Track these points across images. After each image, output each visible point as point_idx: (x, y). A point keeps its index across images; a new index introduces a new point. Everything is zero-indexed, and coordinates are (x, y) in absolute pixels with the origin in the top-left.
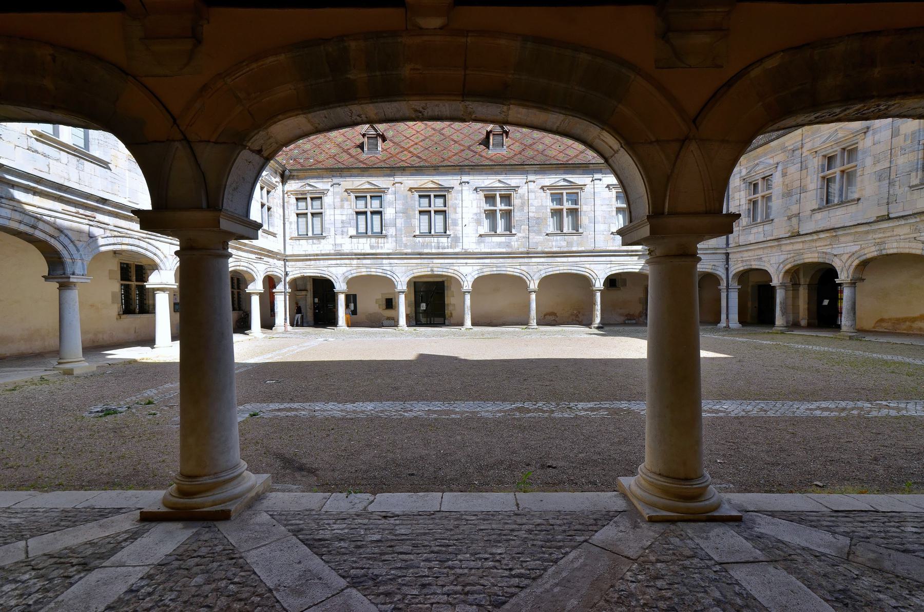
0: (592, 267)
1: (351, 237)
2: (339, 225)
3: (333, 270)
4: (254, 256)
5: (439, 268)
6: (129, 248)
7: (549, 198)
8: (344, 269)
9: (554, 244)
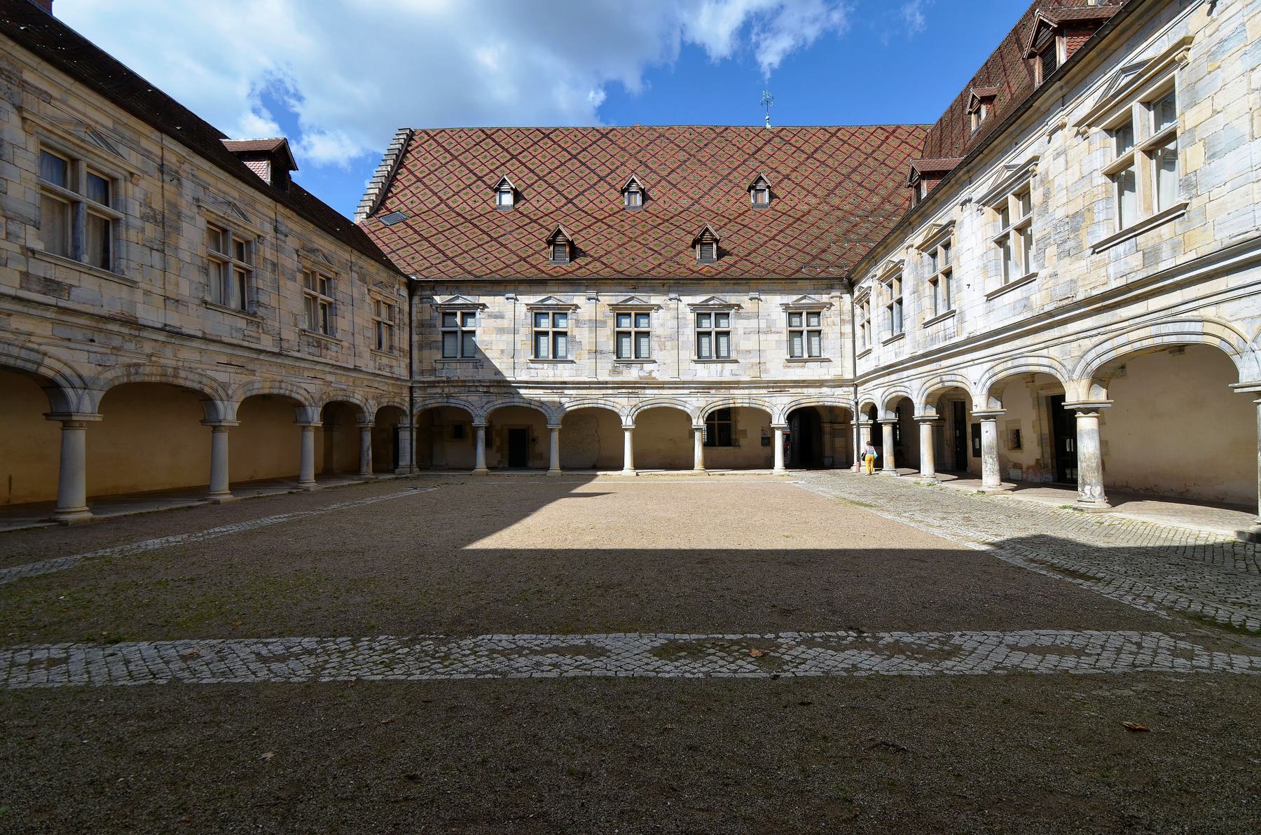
0: (1226, 311)
4: (764, 391)
8: (881, 390)
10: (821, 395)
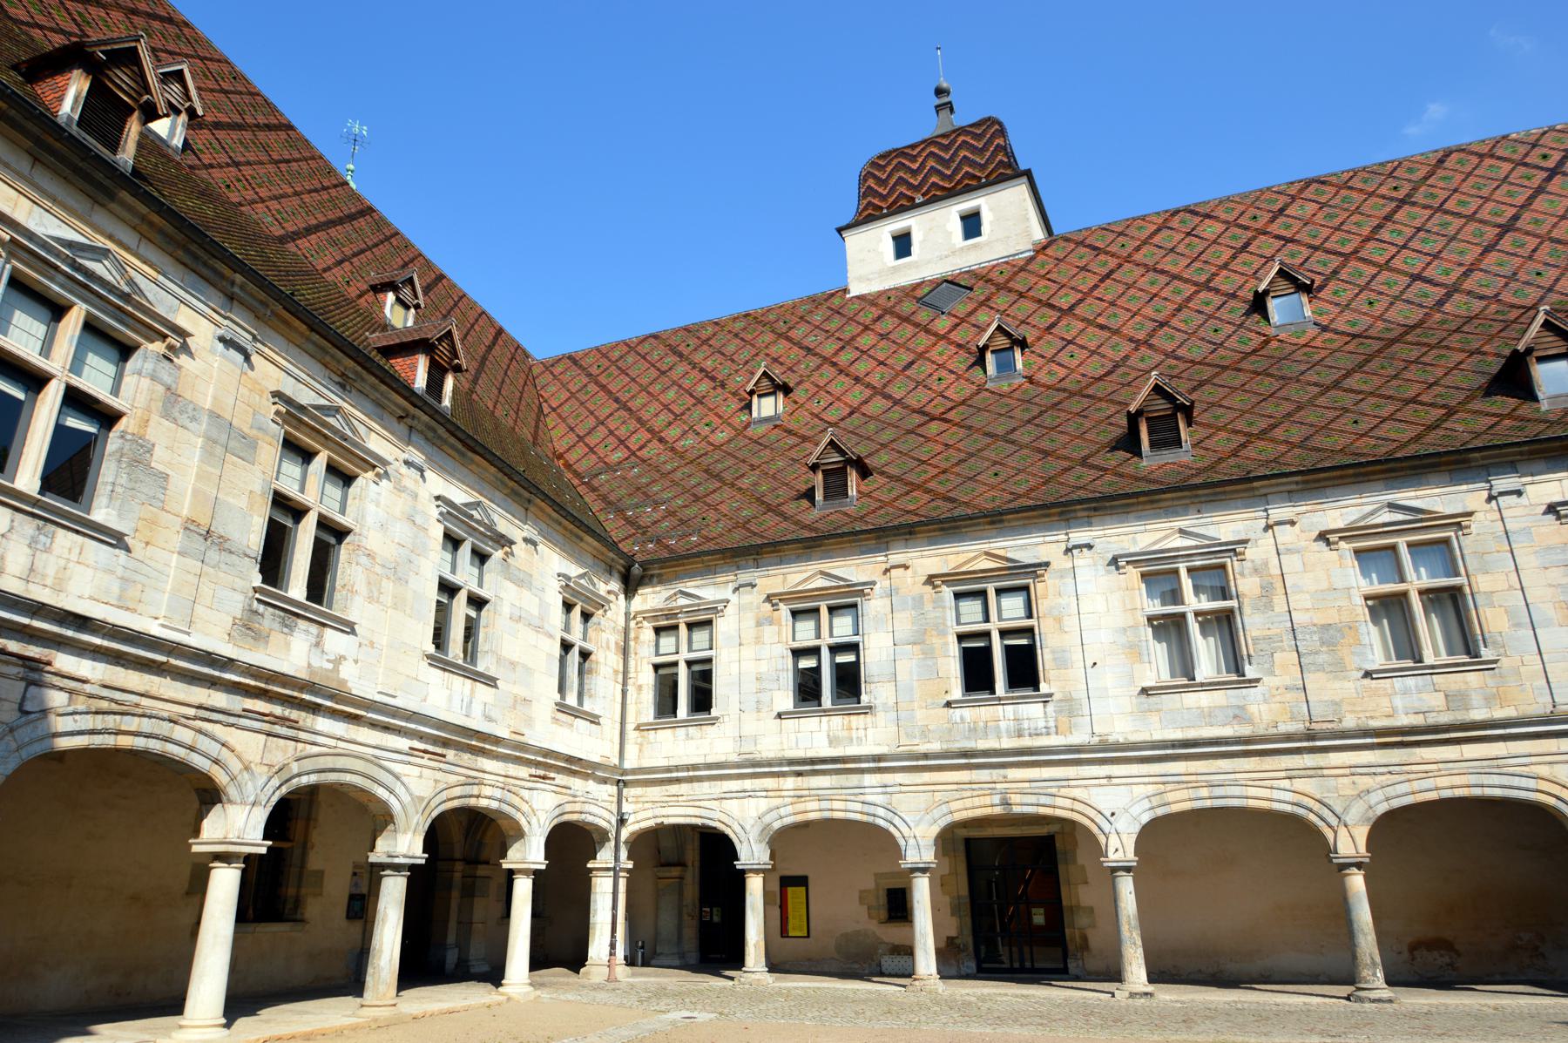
1: (779, 716)
2: (750, 686)
3: (732, 806)
4: (524, 772)
5: (1031, 794)
6: (140, 743)
7: (1351, 562)
8: (763, 804)
9: (1398, 702)
10: (694, 802)
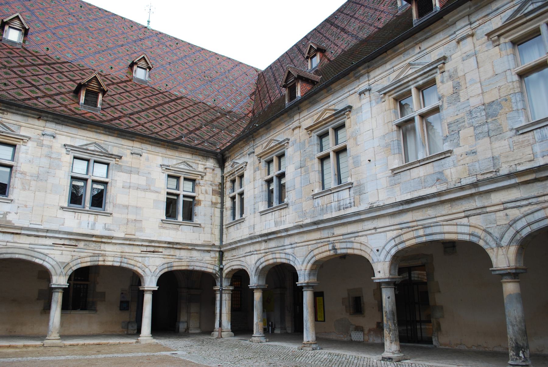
4: (137, 250)
8: (254, 258)
9: (537, 149)
